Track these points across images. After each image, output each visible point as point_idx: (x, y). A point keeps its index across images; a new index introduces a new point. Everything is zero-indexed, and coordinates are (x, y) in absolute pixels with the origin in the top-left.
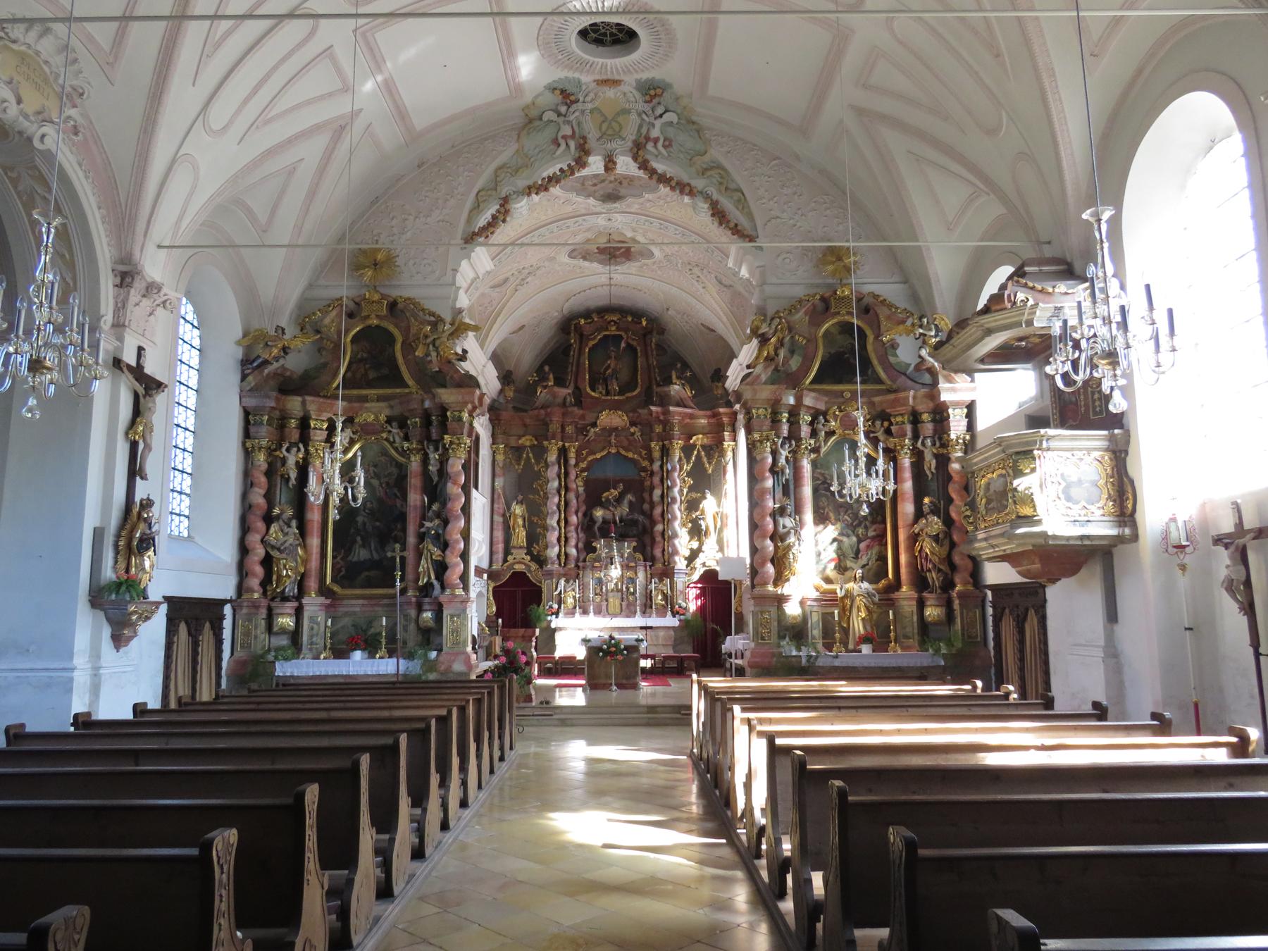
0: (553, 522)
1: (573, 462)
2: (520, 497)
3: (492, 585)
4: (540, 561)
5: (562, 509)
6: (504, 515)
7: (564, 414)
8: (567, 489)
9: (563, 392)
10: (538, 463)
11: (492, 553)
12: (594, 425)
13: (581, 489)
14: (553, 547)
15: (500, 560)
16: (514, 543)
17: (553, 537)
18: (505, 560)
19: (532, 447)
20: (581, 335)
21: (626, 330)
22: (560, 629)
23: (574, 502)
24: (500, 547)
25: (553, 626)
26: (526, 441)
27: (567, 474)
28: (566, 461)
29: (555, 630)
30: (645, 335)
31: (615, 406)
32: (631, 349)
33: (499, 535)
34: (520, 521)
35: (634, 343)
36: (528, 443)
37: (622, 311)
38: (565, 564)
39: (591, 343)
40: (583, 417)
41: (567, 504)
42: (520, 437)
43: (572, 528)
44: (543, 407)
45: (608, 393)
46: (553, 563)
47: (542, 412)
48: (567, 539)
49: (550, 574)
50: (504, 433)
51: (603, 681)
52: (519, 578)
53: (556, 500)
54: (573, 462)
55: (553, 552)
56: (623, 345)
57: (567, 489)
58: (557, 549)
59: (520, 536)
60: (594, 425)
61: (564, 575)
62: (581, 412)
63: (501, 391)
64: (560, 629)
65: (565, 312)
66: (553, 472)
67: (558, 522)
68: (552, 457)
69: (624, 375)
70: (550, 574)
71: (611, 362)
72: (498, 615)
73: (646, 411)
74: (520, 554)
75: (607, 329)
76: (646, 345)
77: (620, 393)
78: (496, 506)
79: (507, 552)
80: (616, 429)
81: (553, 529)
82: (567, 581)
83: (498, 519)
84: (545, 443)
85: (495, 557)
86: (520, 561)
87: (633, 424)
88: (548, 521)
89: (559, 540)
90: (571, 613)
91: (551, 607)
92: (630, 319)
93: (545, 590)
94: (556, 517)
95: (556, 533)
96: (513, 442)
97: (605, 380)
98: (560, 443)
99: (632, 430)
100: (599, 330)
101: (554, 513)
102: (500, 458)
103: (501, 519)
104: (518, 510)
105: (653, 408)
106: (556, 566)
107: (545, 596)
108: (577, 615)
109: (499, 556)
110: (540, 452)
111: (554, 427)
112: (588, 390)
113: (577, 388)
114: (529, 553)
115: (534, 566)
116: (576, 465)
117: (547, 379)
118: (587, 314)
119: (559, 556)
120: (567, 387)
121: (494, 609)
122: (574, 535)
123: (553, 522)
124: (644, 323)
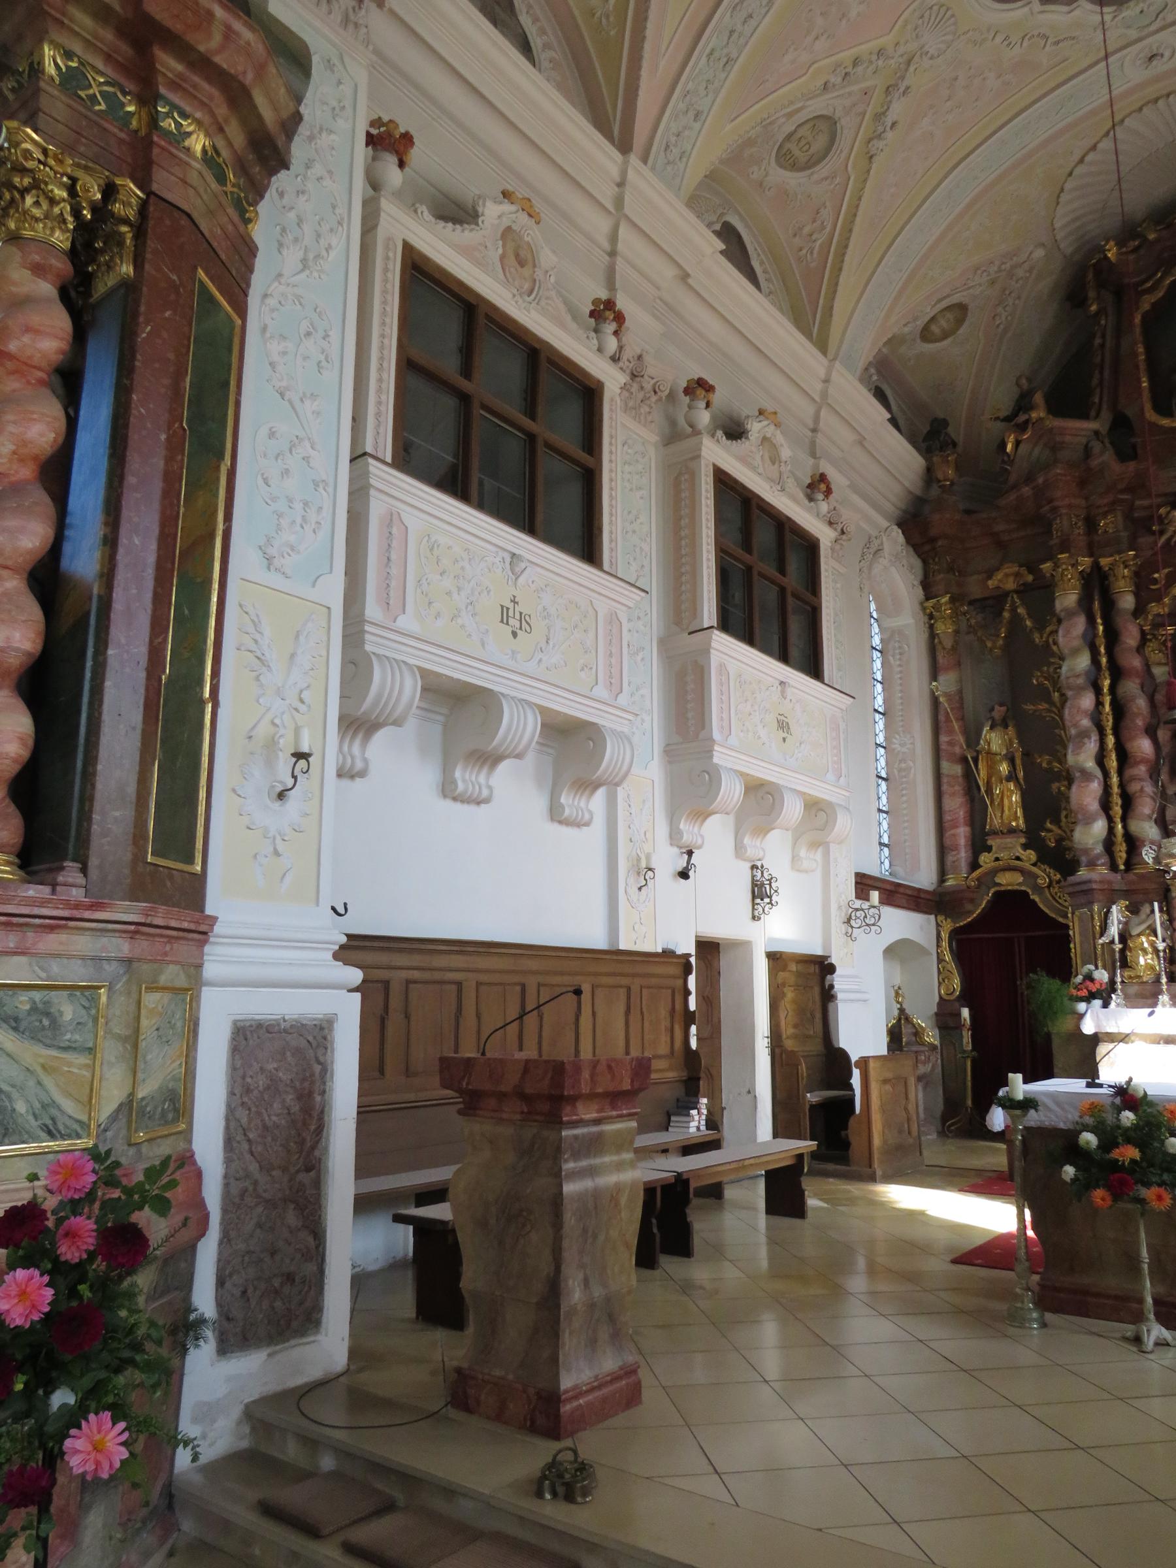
0: (1084, 757)
1: (1127, 602)
2: (999, 712)
3: (948, 926)
4: (1062, 860)
5: (1109, 724)
6: (964, 760)
7: (1082, 483)
8: (1117, 673)
9: (1077, 430)
10: (1041, 626)
11: (943, 850)
13: (1160, 672)
14: (1089, 820)
15: (964, 866)
16: (995, 820)
17: (1087, 795)
18: (974, 865)
19: (1023, 591)
22: (1113, 1038)
23: (1141, 704)
24: (961, 834)
25: (1088, 1028)
26: (1005, 579)
27: (1113, 637)
28: (1109, 606)
29: (1096, 1039)
33: (956, 805)
34: (1004, 768)
36: (1010, 585)
38: (1129, 865)
40: (1138, 486)
41: (1119, 710)
42: (990, 575)
43: (1142, 770)
44: (1029, 478)
46: (1092, 864)
47: (1026, 490)
48: (1128, 802)
49: (1084, 894)
50: (951, 570)
51: (1111, 1282)
52: (1012, 906)
53: (1087, 701)
54: (1127, 602)
55: (1092, 833)
57: (1117, 673)
58: (1099, 827)
59: (1009, 804)
61: (1126, 894)
62: (1132, 466)
63: (929, 474)
64: (1113, 1038)
65: (1067, 247)
66: (1072, 634)
67: (1100, 760)
68: (1067, 599)
70: (1084, 894)
72: (968, 996)
74: (1010, 849)
78: (944, 739)
79: (979, 845)
81: (1087, 776)
82: (1134, 909)
83: (953, 769)
84: (1047, 566)
85: (950, 859)
86: (1013, 864)
88: (1071, 759)
89: (1106, 806)
90: (1147, 997)
91: (1089, 977)
93: (1075, 932)
94: (1092, 746)
95: (1095, 787)
96: (976, 592)
98: (1085, 562)
101: (1084, 735)
102: (945, 628)
103: (958, 769)
104: (995, 740)
106: (1103, 871)
107: (1076, 948)
108: (1164, 998)
109: (963, 855)
110: (1040, 593)
111: (1068, 522)
112: (1151, 415)
114: (1033, 841)
115: (1044, 874)
116: (1139, 611)
117: (1031, 407)
118: (1129, 233)
119: (1109, 844)
120: (1085, 416)
121: (957, 982)
122: (1149, 788)
123: (1084, 757)
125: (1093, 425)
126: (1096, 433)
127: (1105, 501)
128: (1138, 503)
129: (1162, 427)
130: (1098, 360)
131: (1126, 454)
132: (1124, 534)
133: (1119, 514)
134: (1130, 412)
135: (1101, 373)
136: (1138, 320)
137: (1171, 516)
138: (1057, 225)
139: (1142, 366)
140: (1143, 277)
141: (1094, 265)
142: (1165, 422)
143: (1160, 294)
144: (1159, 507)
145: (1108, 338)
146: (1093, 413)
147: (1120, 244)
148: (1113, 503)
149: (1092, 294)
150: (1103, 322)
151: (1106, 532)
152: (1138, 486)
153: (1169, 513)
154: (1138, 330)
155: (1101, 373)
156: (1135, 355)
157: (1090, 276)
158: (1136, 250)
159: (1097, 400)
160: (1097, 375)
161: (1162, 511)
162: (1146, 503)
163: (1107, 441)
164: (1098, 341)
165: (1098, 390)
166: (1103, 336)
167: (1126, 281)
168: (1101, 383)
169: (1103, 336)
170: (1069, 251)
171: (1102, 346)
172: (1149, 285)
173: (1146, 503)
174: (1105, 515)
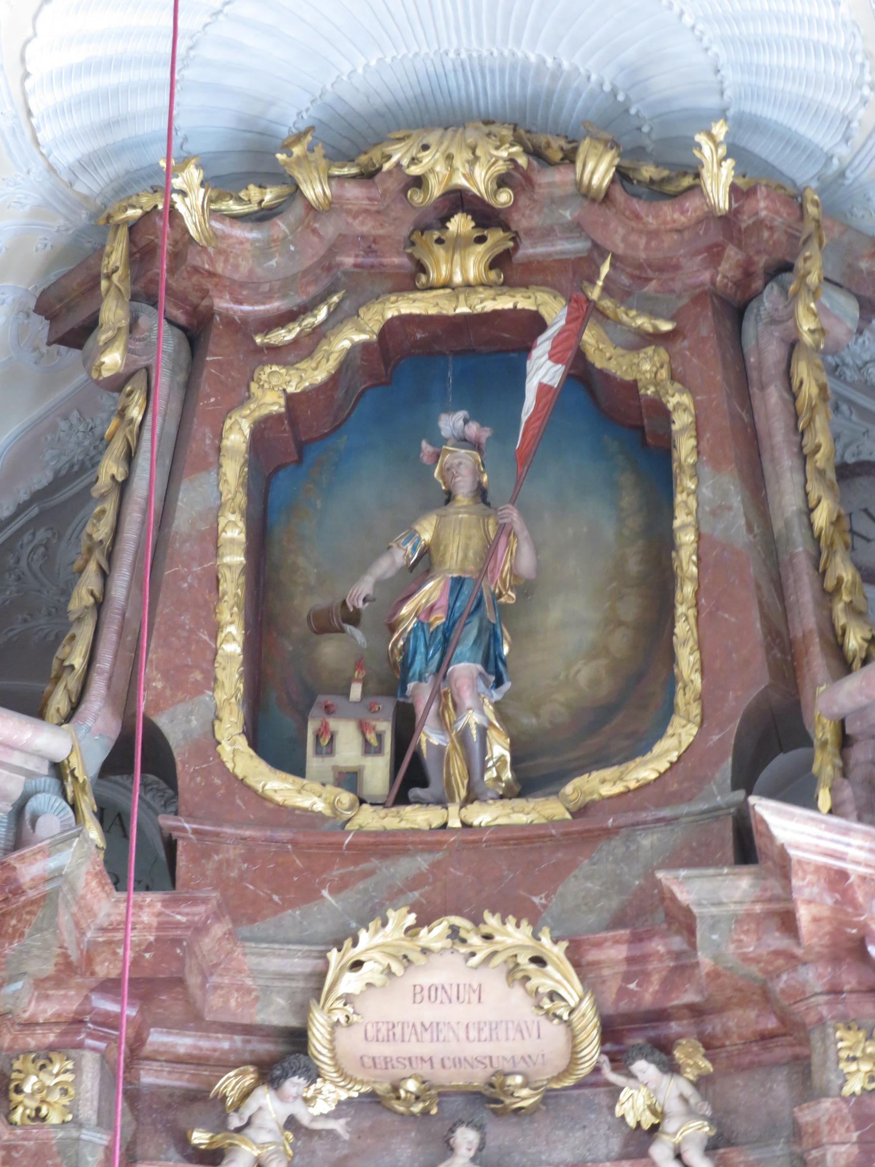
12: (286, 1054)
20: (196, 331)
21: (569, 277)
30: (734, 309)
31: (470, 885)
32: (618, 425)
35: (646, 368)
37: (540, 139)
39: (273, 390)
40: (159, 983)
45: (411, 778)
56: (543, 370)
60: (286, 1054)
62: (150, 908)
69: (570, 645)
71: (454, 536)
73: (738, 887)
75: (413, 278)
76: (742, 382)
77: (527, 782)
80: (486, 1100)
87: (627, 1035)
92: (598, 170)
97: (391, 681)
99: (633, 1106)
100: (346, 283)
105: (785, 824)
113: (141, 757)
118: (253, 162)
120: (34, 708)
124: (718, 184)
125: (48, 740)
126: (58, 769)
127: (49, 1010)
128: (157, 1038)
129: (262, 798)
130: (102, 531)
131: (146, 861)
132: (97, 1138)
133: (90, 1063)
134: (176, 727)
135: (105, 576)
136: (237, 435)
137: (251, 1106)
138: (41, 63)
139: (232, 586)
140: (276, 305)
141: (133, 228)
142: (278, 786)
143: (315, 373)
144: (225, 1064)
145: (143, 461)
146: (59, 702)
147: (221, 184)
148: (77, 1021)
149: (113, 313)
150: (135, 413)
151: (38, 1117)
152: (159, 983)
153: (246, 1095)
154: (233, 470)
155: (105, 576)
156: (212, 541)
157: (117, 255)
158: (263, 216)
159: (78, 661)
160: (90, 581)
161: (230, 1084)
162: (184, 1043)
163: (87, 804)
164: (110, 468)
165: (85, 633)
166: (130, 457)
167: (223, 304)
168: (100, 605)
169: (130, 457)
170: (66, 157)
171: (123, 487)
172: (284, 336)
173: (184, 1043)
174: (44, 1057)
